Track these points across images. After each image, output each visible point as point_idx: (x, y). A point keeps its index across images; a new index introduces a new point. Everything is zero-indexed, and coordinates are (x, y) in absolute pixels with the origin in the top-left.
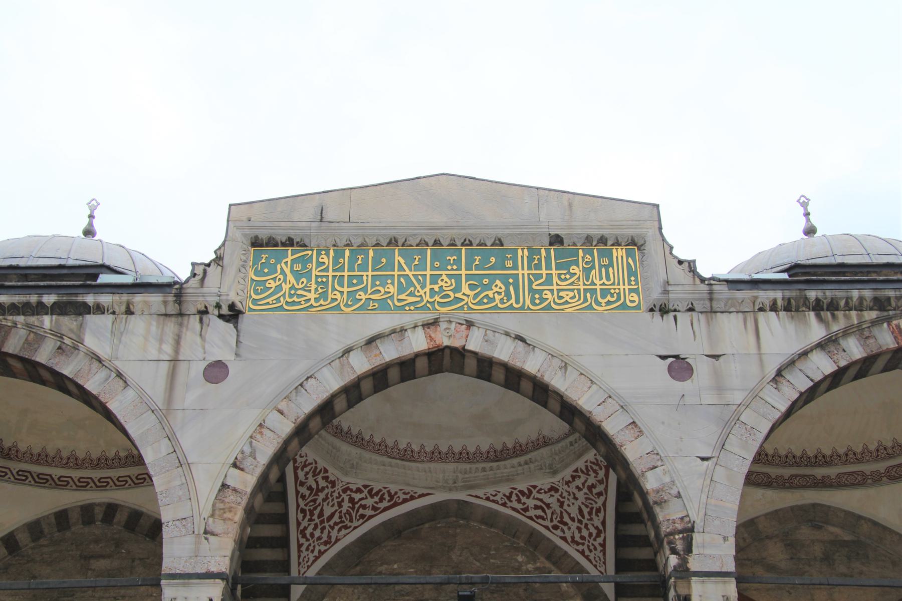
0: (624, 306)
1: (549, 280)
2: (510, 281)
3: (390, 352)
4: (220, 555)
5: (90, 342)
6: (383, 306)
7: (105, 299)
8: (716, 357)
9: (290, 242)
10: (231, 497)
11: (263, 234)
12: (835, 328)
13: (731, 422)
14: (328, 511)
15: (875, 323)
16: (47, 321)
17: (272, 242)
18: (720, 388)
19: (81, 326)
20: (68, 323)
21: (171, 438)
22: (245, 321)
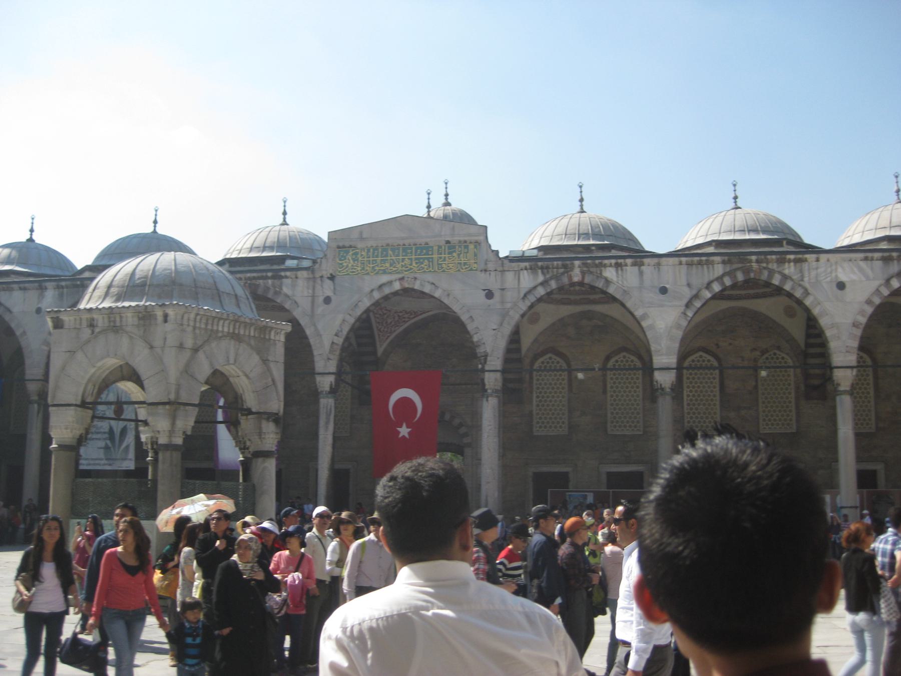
0: (471, 270)
1: (444, 260)
2: (430, 260)
3: (387, 291)
4: (332, 367)
5: (285, 290)
6: (384, 272)
7: (288, 274)
8: (503, 289)
9: (350, 247)
10: (335, 347)
11: (341, 244)
12: (548, 276)
13: (504, 315)
14: (389, 321)
15: (563, 274)
16: (270, 281)
17: (344, 247)
18: (503, 302)
19: (281, 283)
20: (277, 282)
21: (315, 325)
22: (337, 280)
